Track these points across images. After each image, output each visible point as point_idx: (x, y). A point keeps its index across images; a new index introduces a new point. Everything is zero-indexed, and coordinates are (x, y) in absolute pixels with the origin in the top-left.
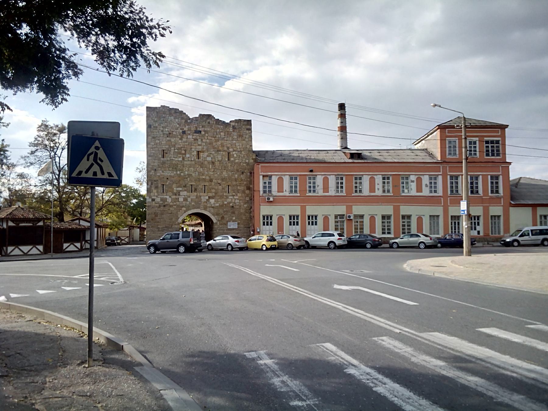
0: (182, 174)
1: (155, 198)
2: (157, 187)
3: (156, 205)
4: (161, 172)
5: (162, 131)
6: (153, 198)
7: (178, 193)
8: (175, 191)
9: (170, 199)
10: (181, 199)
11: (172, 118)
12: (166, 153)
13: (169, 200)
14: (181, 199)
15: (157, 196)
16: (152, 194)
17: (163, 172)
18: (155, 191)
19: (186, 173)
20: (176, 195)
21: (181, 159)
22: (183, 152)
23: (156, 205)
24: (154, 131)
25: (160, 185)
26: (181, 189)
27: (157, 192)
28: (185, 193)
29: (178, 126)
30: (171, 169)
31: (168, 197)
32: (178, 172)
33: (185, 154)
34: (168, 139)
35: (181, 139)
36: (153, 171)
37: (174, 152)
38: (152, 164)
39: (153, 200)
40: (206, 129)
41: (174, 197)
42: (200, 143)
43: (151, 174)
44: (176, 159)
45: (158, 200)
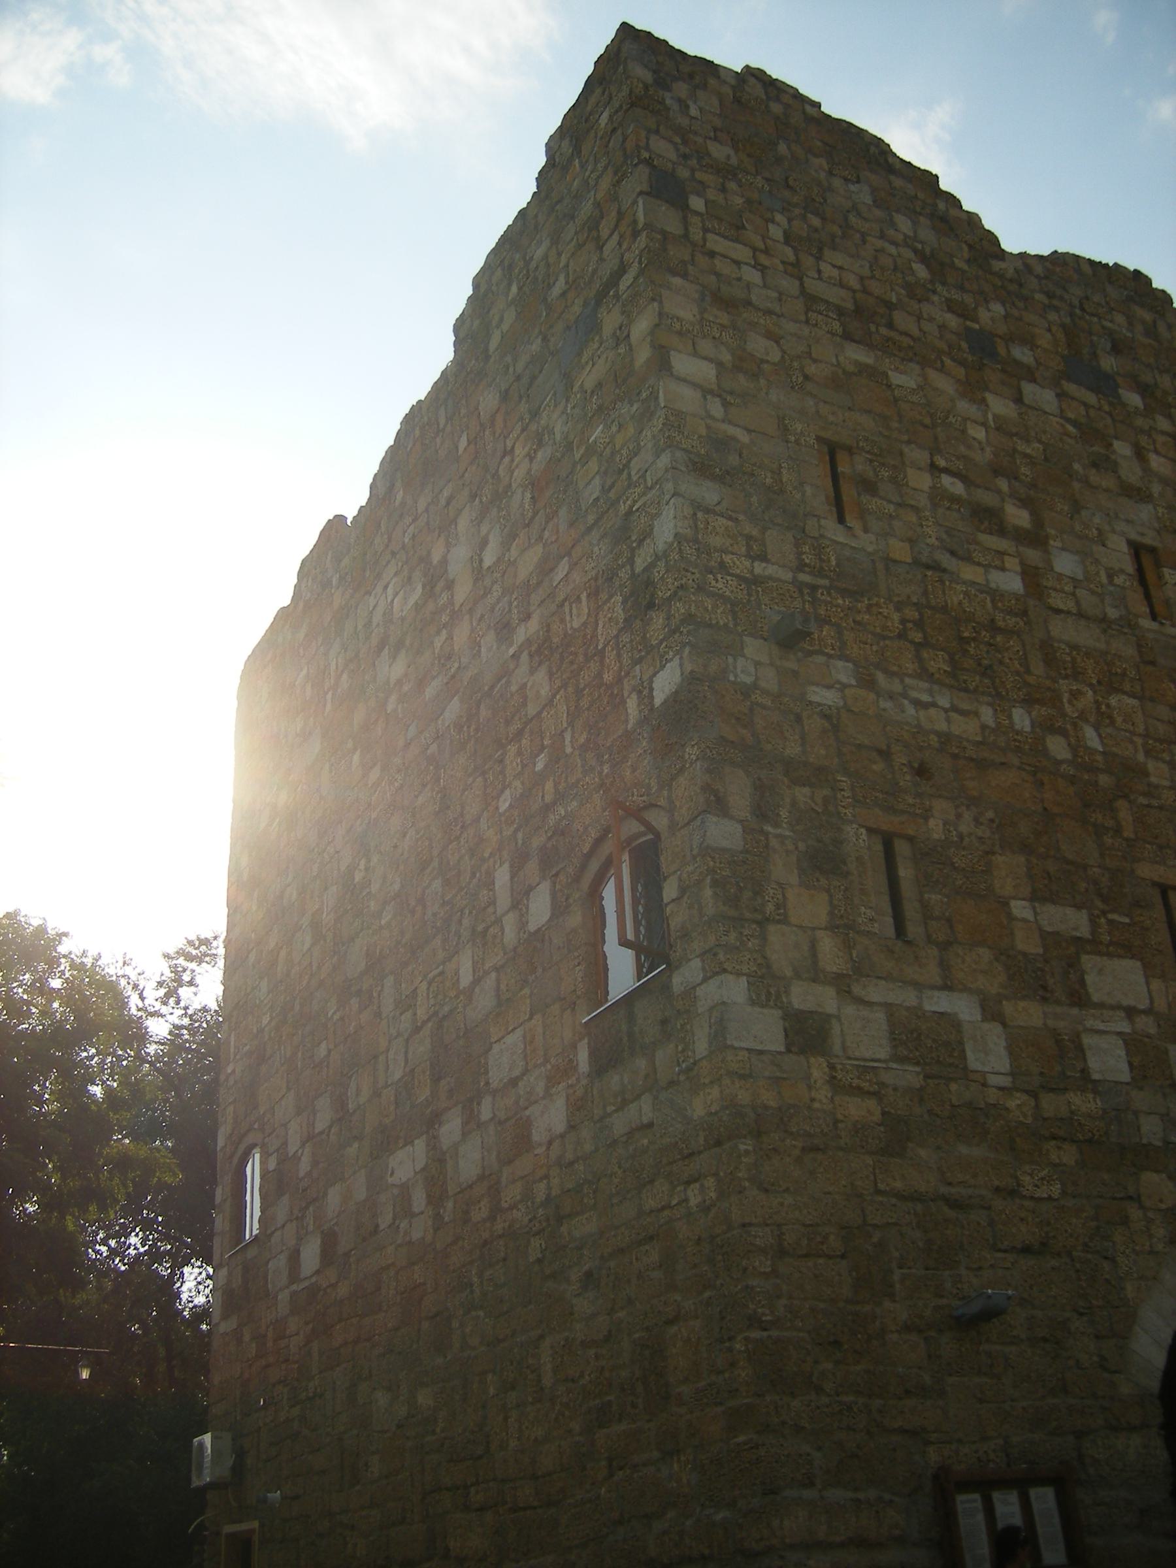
0: (1057, 747)
1: (825, 999)
2: (823, 863)
3: (857, 1109)
4: (842, 672)
5: (795, 270)
6: (802, 996)
7: (1052, 975)
8: (1027, 944)
9: (995, 1037)
10: (1108, 1060)
11: (864, 196)
12: (869, 486)
13: (990, 1057)
14: (1108, 1060)
15: (842, 984)
16: (782, 947)
17: (868, 683)
18: (810, 907)
19: (1091, 737)
20: (1043, 994)
21: (1011, 583)
22: (1018, 517)
23: (857, 1109)
24: (716, 243)
25: (857, 841)
26: (1075, 922)
27: (842, 926)
28: (1117, 980)
29: (921, 271)
30: (938, 663)
31: (964, 1008)
32: (1021, 719)
33: (1035, 538)
34: (856, 354)
35: (973, 389)
36: (754, 648)
37: (938, 496)
38: (742, 565)
39: (807, 1033)
40: (1147, 377)
41: (1029, 1014)
42: (1131, 472)
43: (743, 672)
44: (969, 573)
45: (863, 1036)
